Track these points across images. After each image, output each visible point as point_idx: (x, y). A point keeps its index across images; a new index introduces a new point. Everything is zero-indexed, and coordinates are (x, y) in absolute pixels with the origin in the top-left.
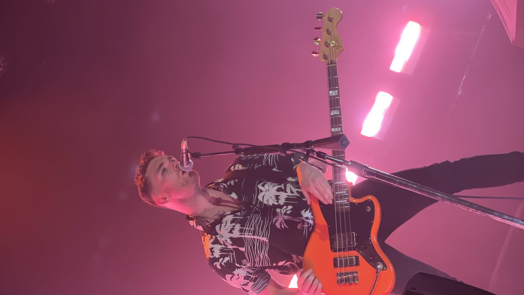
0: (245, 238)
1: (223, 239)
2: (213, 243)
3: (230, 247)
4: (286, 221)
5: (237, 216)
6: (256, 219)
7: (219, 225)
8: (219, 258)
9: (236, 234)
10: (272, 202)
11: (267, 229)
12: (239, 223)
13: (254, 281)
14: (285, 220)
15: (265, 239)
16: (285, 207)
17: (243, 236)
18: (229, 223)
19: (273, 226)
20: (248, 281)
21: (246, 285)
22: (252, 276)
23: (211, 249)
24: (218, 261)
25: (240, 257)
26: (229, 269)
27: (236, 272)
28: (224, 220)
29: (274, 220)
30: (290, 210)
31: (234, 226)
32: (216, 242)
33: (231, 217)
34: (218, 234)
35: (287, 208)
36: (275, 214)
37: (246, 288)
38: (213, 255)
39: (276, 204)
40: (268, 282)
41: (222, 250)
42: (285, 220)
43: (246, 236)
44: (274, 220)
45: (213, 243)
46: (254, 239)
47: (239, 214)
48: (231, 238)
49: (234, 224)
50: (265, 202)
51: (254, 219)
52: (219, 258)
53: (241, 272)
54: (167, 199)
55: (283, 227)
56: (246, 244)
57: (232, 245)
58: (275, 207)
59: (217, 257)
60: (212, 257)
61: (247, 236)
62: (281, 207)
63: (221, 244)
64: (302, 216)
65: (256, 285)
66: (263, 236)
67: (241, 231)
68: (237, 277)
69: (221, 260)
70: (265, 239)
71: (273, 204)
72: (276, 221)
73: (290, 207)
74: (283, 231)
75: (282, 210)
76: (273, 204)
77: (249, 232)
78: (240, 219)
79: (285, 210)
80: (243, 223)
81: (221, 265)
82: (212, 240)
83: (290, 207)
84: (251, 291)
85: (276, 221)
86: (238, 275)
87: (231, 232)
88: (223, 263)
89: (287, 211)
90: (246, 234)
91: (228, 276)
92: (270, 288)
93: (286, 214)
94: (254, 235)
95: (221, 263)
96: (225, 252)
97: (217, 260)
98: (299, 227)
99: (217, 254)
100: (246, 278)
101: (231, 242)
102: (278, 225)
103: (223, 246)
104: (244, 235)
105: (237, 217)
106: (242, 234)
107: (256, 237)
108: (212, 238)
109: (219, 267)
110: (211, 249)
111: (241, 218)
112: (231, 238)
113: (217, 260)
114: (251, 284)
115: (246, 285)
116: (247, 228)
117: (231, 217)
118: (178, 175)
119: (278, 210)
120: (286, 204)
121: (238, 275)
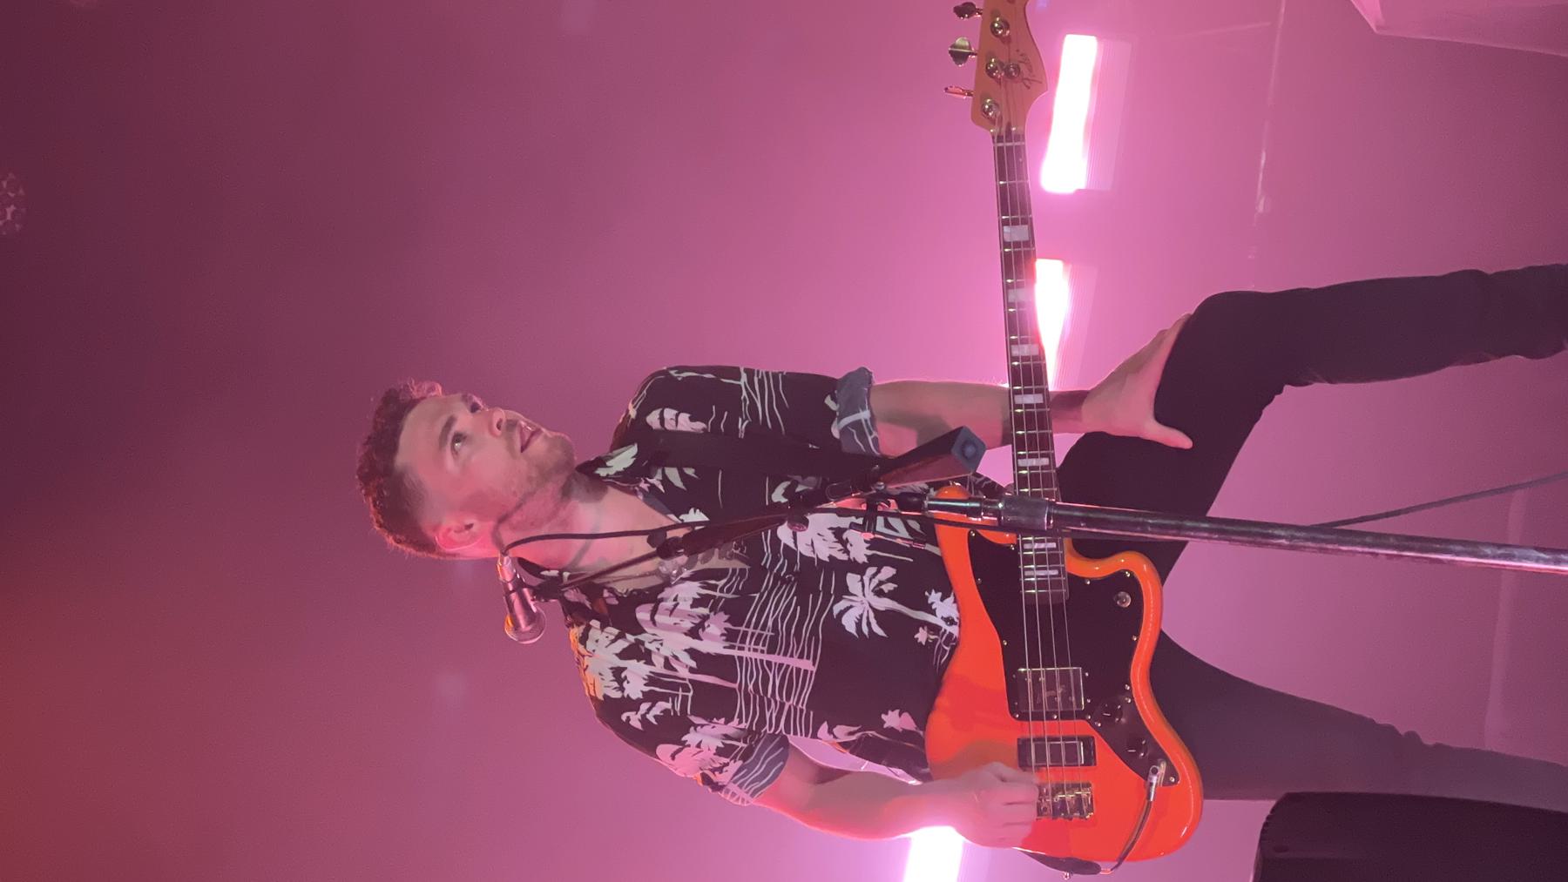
0: (740, 658)
1: (666, 652)
2: (623, 655)
3: (683, 673)
4: (882, 617)
5: (714, 588)
6: (776, 606)
7: (650, 607)
8: (638, 702)
9: (713, 644)
10: (826, 549)
11: (814, 632)
12: (725, 609)
13: (746, 755)
14: (875, 610)
15: (807, 665)
16: (871, 571)
17: (735, 653)
18: (685, 606)
19: (835, 623)
20: (726, 760)
21: (720, 770)
22: (741, 744)
23: (618, 673)
24: (637, 710)
25: (714, 704)
26: (672, 729)
27: (691, 738)
28: (668, 593)
29: (837, 609)
30: (890, 580)
31: (705, 618)
32: (637, 652)
33: (692, 589)
34: (638, 629)
35: (878, 572)
36: (843, 591)
37: (720, 778)
38: (622, 689)
39: (843, 557)
40: (783, 758)
41: (653, 680)
42: (875, 610)
43: (745, 654)
44: (837, 609)
45: (623, 655)
46: (769, 663)
47: (721, 583)
48: (692, 653)
49: (704, 611)
50: (804, 549)
51: (771, 606)
52: (638, 702)
53: (707, 737)
54: (474, 529)
55: (865, 630)
56: (741, 675)
57: (692, 670)
58: (841, 568)
59: (634, 697)
60: (617, 695)
61: (749, 653)
62: (859, 569)
63: (649, 662)
64: (933, 612)
65: (750, 768)
66: (801, 657)
67: (730, 636)
68: (693, 749)
69: (644, 707)
70: (807, 665)
71: (830, 557)
72: (842, 613)
73: (887, 572)
74: (866, 641)
75: (866, 579)
76: (830, 557)
77: (757, 643)
78: (727, 600)
79: (875, 581)
80: (736, 611)
81: (644, 720)
82: (621, 645)
83: (887, 572)
84: (733, 788)
85: (842, 613)
86: (698, 746)
87: (694, 633)
88: (650, 717)
89: (881, 583)
90: (746, 646)
91: (664, 750)
92: (791, 781)
93: (879, 593)
94: (771, 651)
95: (644, 716)
96: (660, 685)
97: (633, 705)
98: (922, 636)
99: (635, 689)
100: (720, 752)
101: (693, 664)
102: (849, 623)
103: (659, 667)
104: (741, 649)
105: (718, 594)
106: (732, 647)
107: (775, 659)
108: (618, 637)
109: (635, 722)
110: (618, 673)
111: (730, 596)
112: (692, 653)
113: (633, 705)
114: (734, 766)
115: (720, 770)
116: (750, 630)
117: (692, 589)
118: (510, 448)
119: (852, 580)
120: (873, 561)
121: (698, 746)
